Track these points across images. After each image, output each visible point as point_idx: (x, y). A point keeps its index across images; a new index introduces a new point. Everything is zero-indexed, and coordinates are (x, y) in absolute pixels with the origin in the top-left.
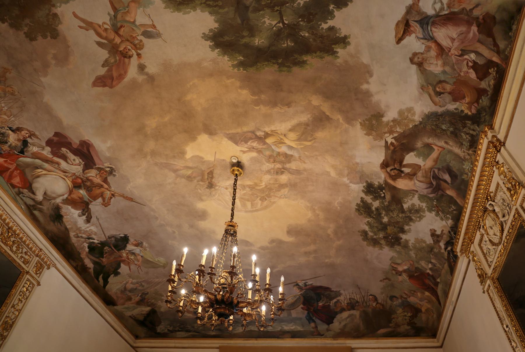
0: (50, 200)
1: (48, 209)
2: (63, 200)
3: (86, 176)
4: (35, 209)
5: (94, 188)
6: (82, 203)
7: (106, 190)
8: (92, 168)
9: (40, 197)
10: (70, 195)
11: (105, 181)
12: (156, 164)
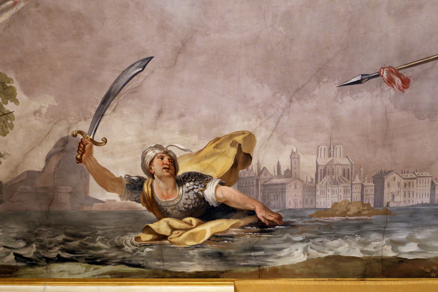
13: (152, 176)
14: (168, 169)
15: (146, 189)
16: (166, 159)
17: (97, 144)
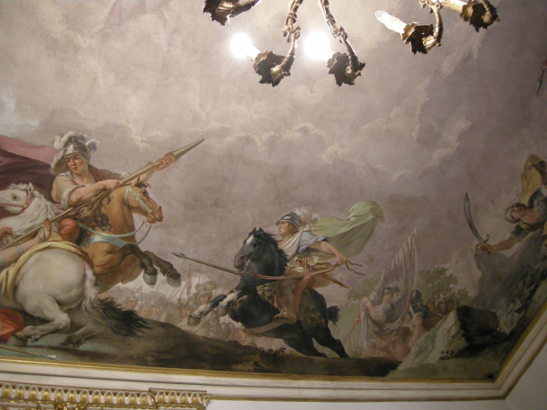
0: (80, 306)
1: (96, 322)
2: (96, 284)
3: (64, 203)
4: (79, 343)
5: (103, 210)
6: (124, 256)
7: (122, 190)
8: (52, 178)
9: (61, 318)
10: (92, 266)
11: (97, 175)
12: (105, 37)
13: (519, 220)
14: (521, 210)
15: (523, 226)
16: (515, 208)
17: (487, 240)
